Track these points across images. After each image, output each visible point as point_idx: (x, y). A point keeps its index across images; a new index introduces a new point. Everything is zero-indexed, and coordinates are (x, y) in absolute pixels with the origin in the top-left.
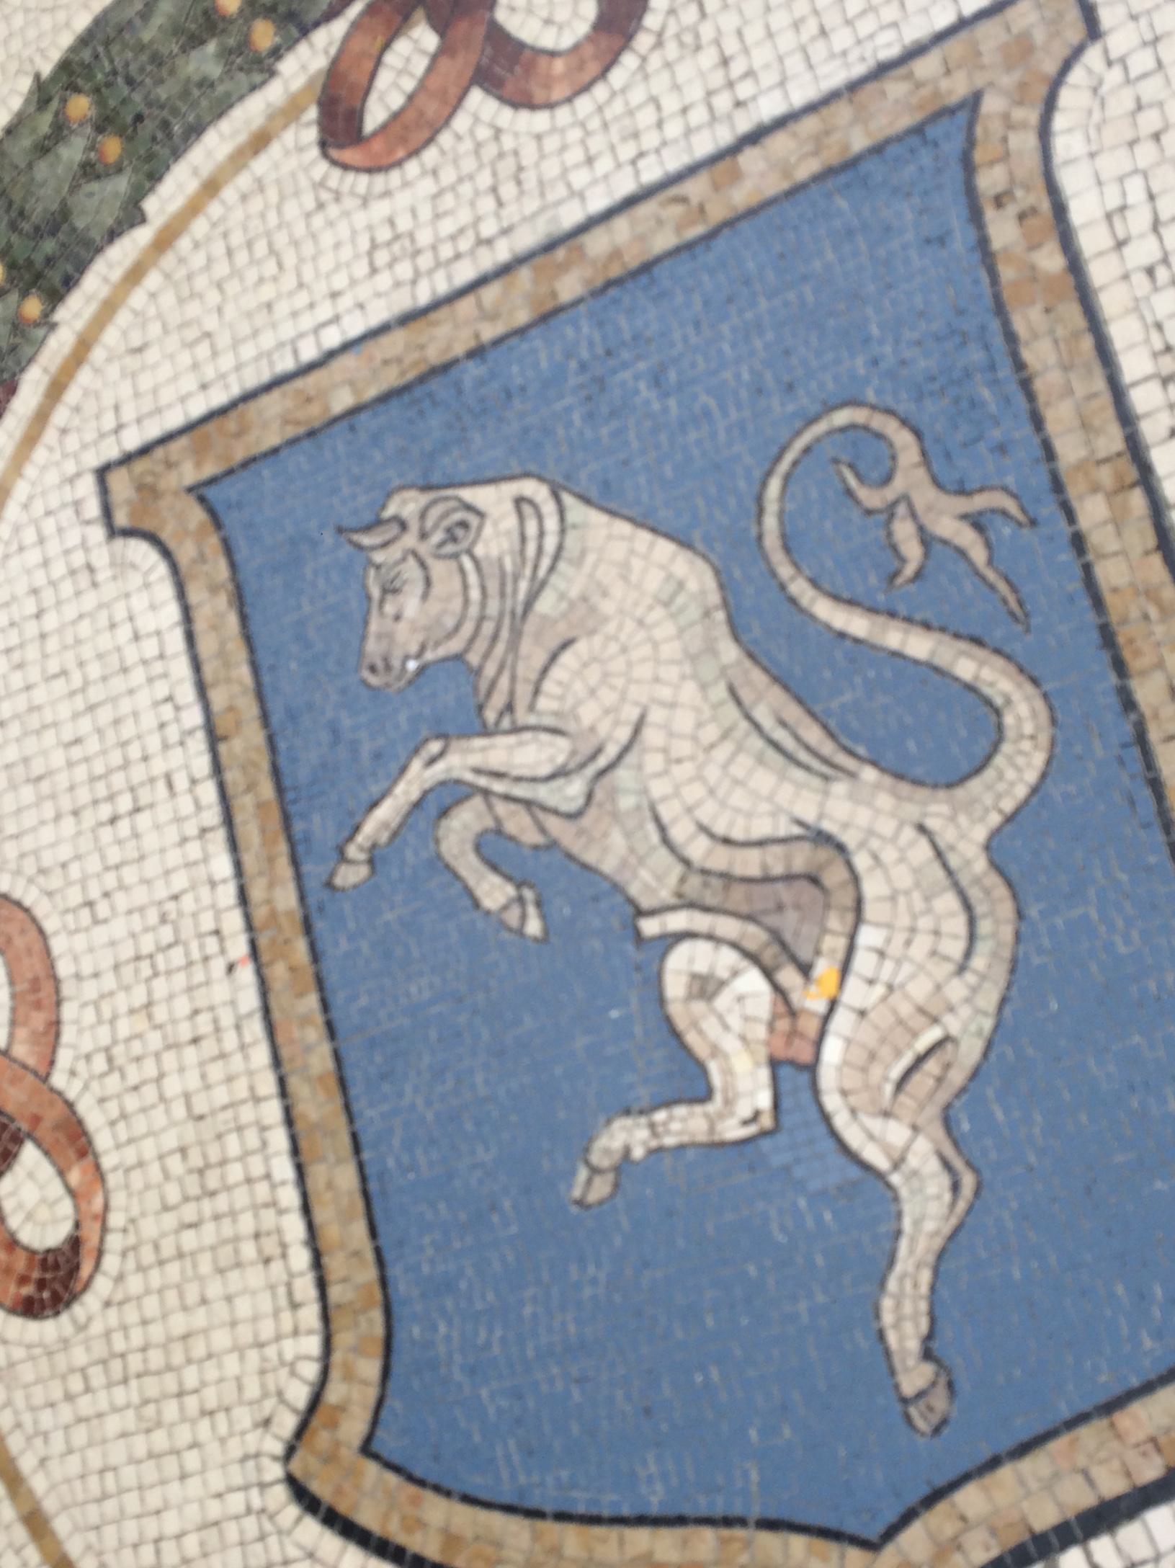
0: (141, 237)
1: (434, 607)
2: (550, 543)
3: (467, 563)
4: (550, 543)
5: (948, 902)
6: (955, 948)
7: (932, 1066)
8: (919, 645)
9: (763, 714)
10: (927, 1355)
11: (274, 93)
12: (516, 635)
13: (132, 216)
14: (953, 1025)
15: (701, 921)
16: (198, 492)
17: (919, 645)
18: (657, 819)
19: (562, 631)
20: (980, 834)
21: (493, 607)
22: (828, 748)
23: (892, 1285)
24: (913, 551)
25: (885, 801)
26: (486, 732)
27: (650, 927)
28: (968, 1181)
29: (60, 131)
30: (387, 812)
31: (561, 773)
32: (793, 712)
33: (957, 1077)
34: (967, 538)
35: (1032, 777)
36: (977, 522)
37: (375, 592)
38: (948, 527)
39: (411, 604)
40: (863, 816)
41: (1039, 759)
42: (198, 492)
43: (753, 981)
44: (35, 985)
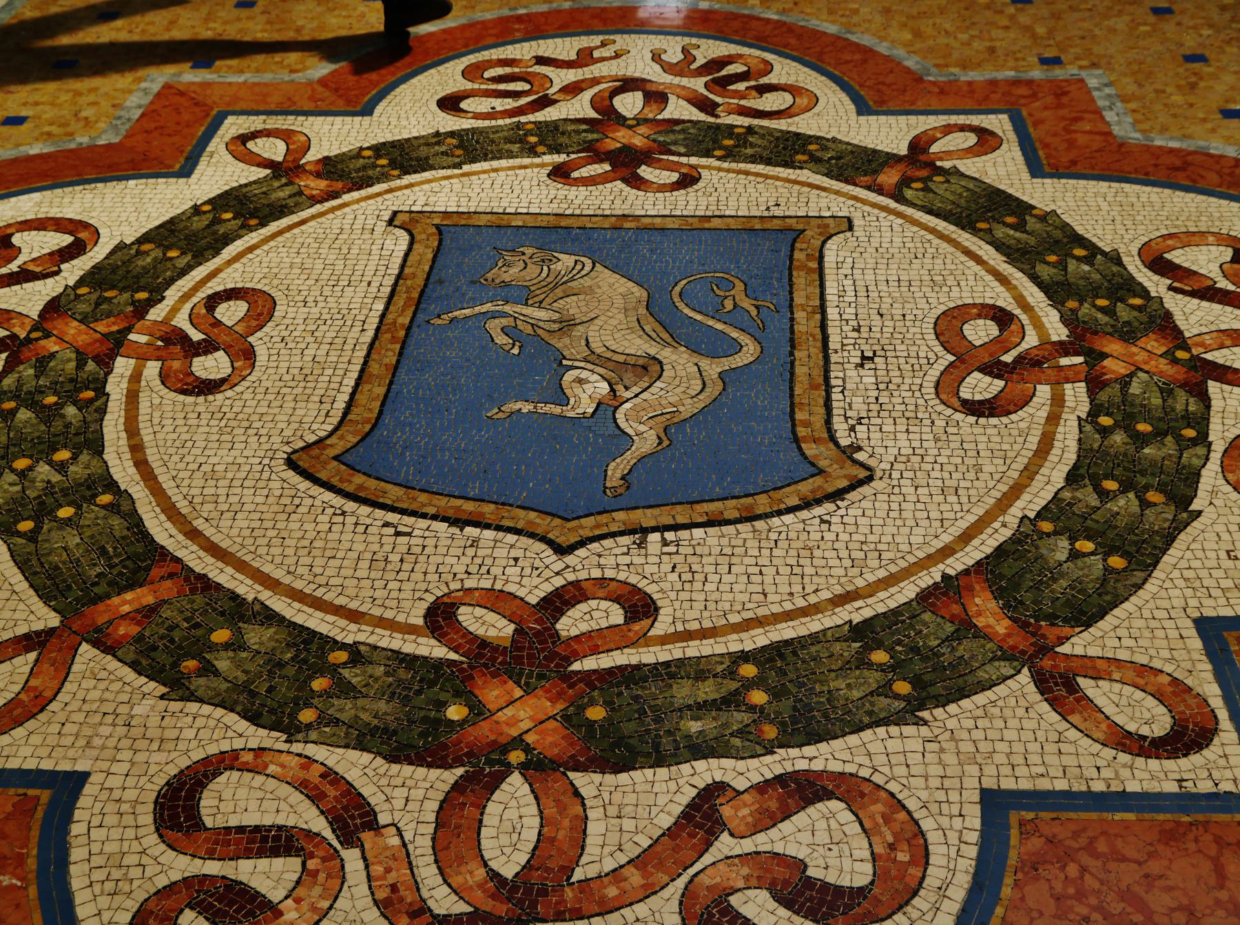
0: (457, 171)
1: (523, 273)
2: (583, 273)
3: (545, 268)
4: (583, 273)
5: (699, 382)
6: (693, 393)
7: (668, 416)
8: (719, 326)
9: (648, 328)
10: (623, 478)
11: (537, 160)
12: (555, 287)
13: (458, 166)
14: (681, 409)
15: (590, 367)
16: (437, 227)
17: (719, 326)
18: (587, 340)
19: (575, 291)
20: (719, 370)
21: (549, 280)
22: (669, 340)
23: (618, 460)
24: (729, 305)
25: (685, 356)
26: (526, 304)
27: (565, 362)
28: (666, 443)
29: (438, 143)
30: (467, 312)
31: (554, 321)
32: (659, 329)
33: (676, 420)
34: (754, 312)
35: (746, 362)
36: (757, 307)
37: (500, 264)
38: (746, 304)
39: (514, 271)
40: (674, 357)
41: (752, 359)
42: (437, 227)
43: (605, 385)
44: (260, 314)
